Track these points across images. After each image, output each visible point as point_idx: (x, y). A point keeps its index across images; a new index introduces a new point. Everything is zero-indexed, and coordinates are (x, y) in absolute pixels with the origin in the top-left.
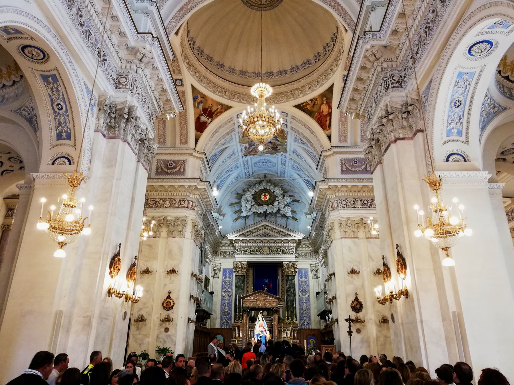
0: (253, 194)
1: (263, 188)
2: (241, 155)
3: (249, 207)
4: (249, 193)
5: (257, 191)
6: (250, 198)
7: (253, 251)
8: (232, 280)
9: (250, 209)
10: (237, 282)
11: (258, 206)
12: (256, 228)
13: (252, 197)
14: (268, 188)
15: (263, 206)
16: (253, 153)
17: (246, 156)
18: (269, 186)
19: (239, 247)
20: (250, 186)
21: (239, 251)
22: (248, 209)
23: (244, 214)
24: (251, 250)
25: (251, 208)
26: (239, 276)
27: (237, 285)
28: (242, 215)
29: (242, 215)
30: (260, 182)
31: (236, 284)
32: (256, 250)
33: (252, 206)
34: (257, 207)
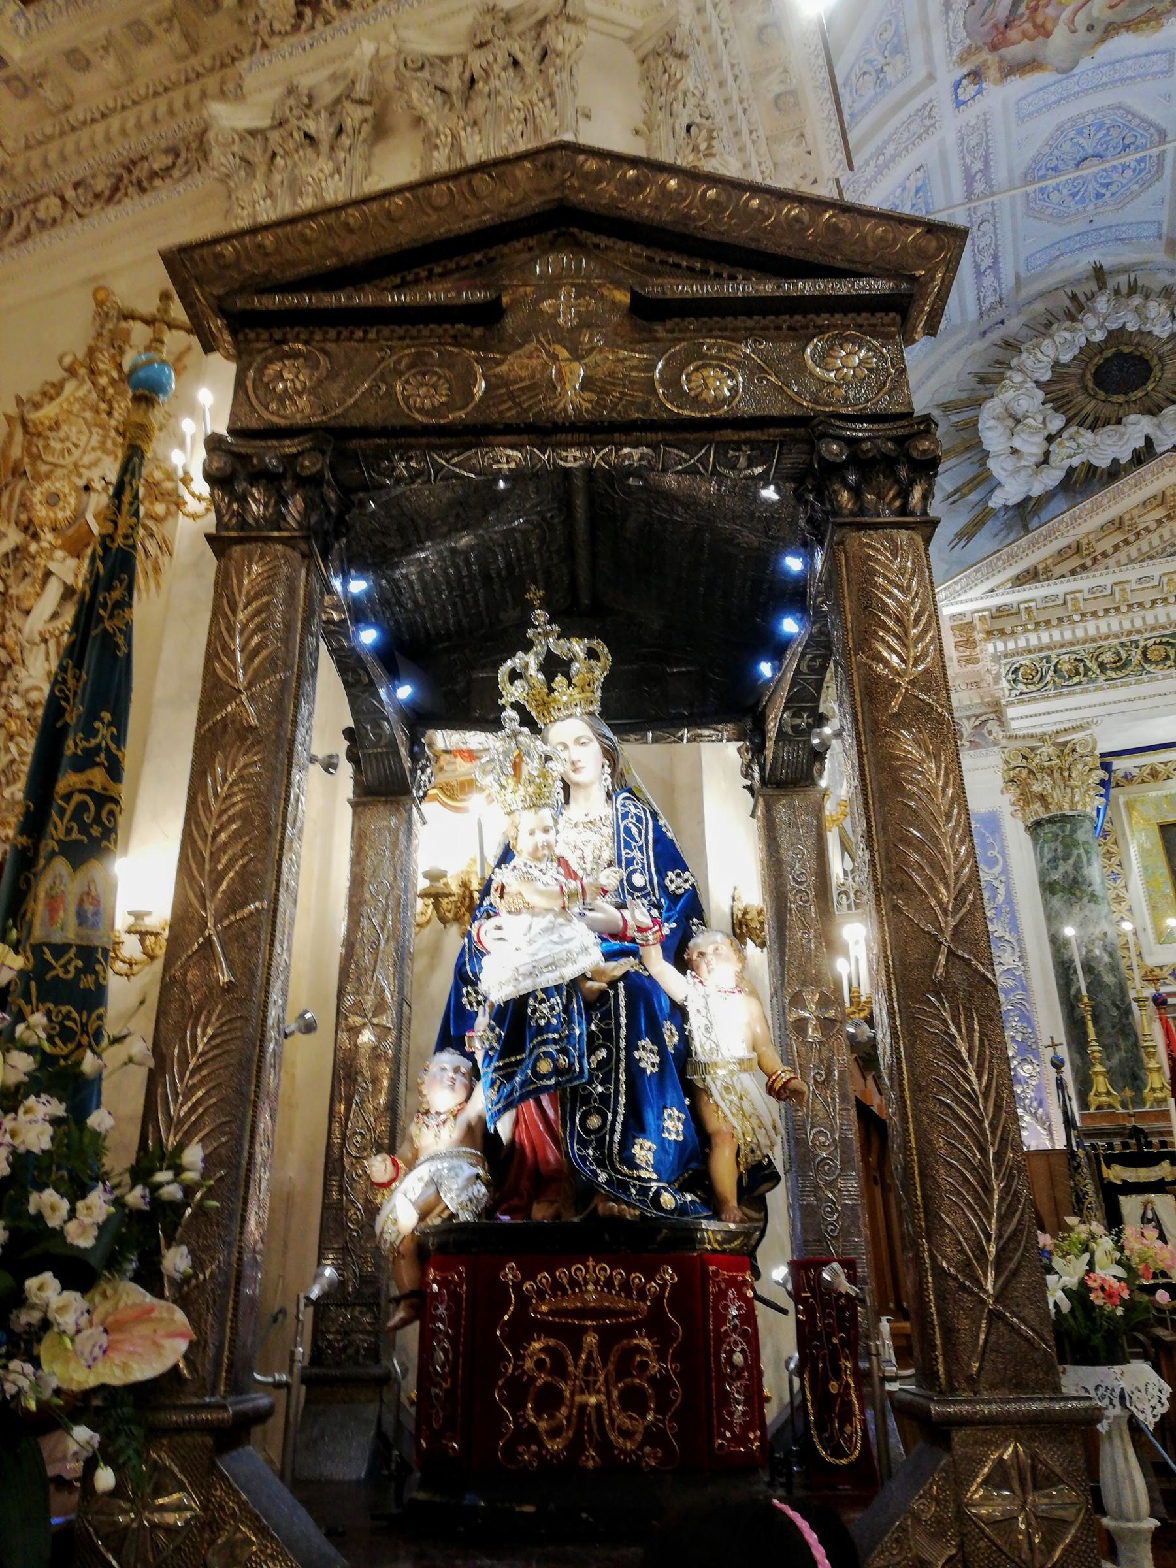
0: (1046, 376)
1: (1099, 336)
2: (948, 73)
3: (1032, 447)
4: (1018, 378)
5: (1065, 358)
6: (1029, 401)
7: (1121, 664)
8: (1005, 871)
9: (1046, 459)
10: (1054, 860)
11: (1093, 428)
12: (1118, 524)
13: (1040, 395)
14: (1131, 327)
15: (1119, 422)
16: (1019, 50)
17: (976, 75)
18: (1139, 311)
19: (1025, 660)
20: (1011, 346)
21: (1029, 681)
22: (1031, 461)
23: (1010, 492)
24: (1107, 657)
25: (1047, 454)
26: (1051, 820)
27: (1056, 876)
28: (996, 501)
29: (996, 501)
30: (1076, 309)
31: (1042, 874)
32: (1136, 656)
33: (1050, 439)
34: (1089, 435)
